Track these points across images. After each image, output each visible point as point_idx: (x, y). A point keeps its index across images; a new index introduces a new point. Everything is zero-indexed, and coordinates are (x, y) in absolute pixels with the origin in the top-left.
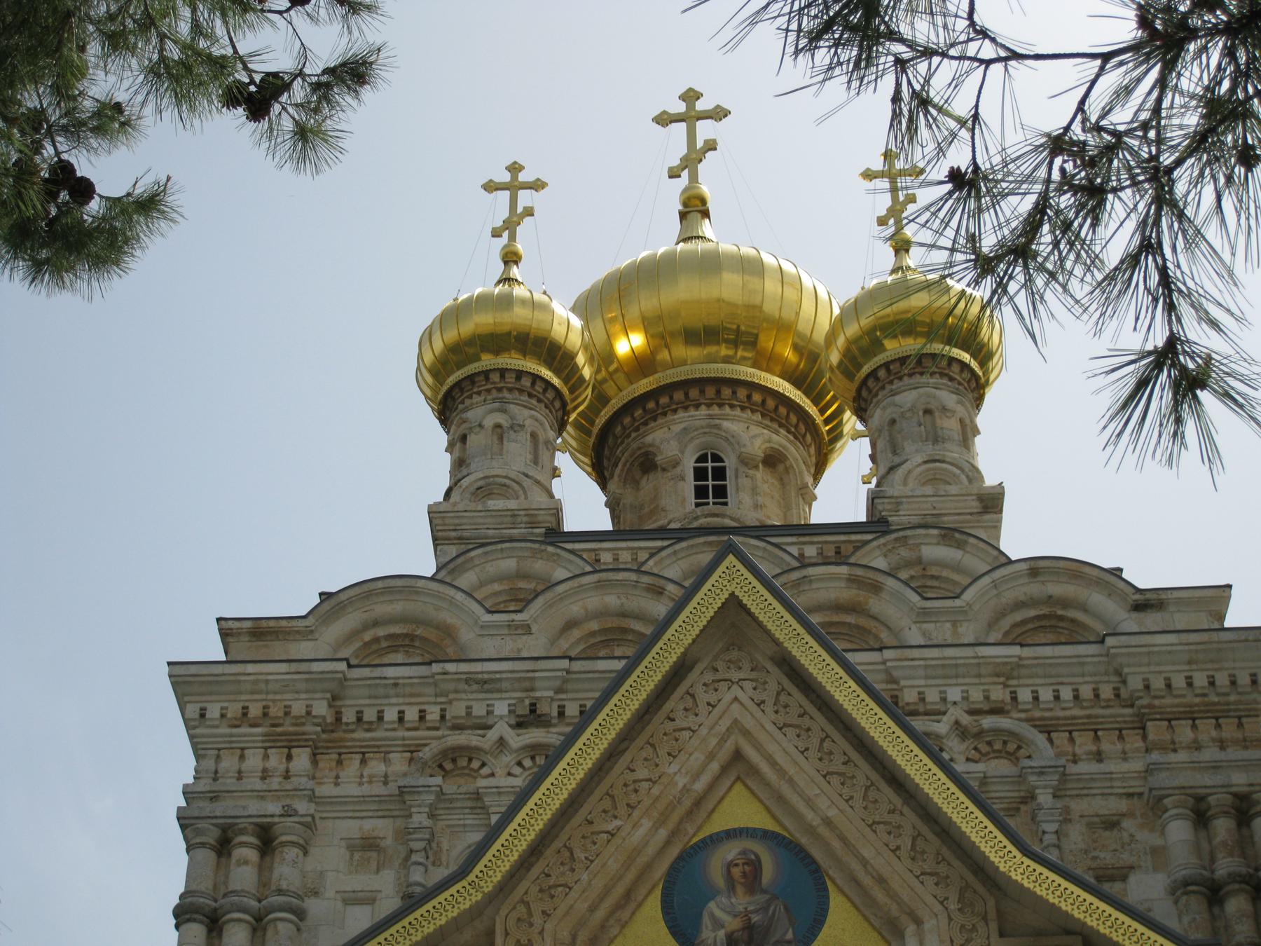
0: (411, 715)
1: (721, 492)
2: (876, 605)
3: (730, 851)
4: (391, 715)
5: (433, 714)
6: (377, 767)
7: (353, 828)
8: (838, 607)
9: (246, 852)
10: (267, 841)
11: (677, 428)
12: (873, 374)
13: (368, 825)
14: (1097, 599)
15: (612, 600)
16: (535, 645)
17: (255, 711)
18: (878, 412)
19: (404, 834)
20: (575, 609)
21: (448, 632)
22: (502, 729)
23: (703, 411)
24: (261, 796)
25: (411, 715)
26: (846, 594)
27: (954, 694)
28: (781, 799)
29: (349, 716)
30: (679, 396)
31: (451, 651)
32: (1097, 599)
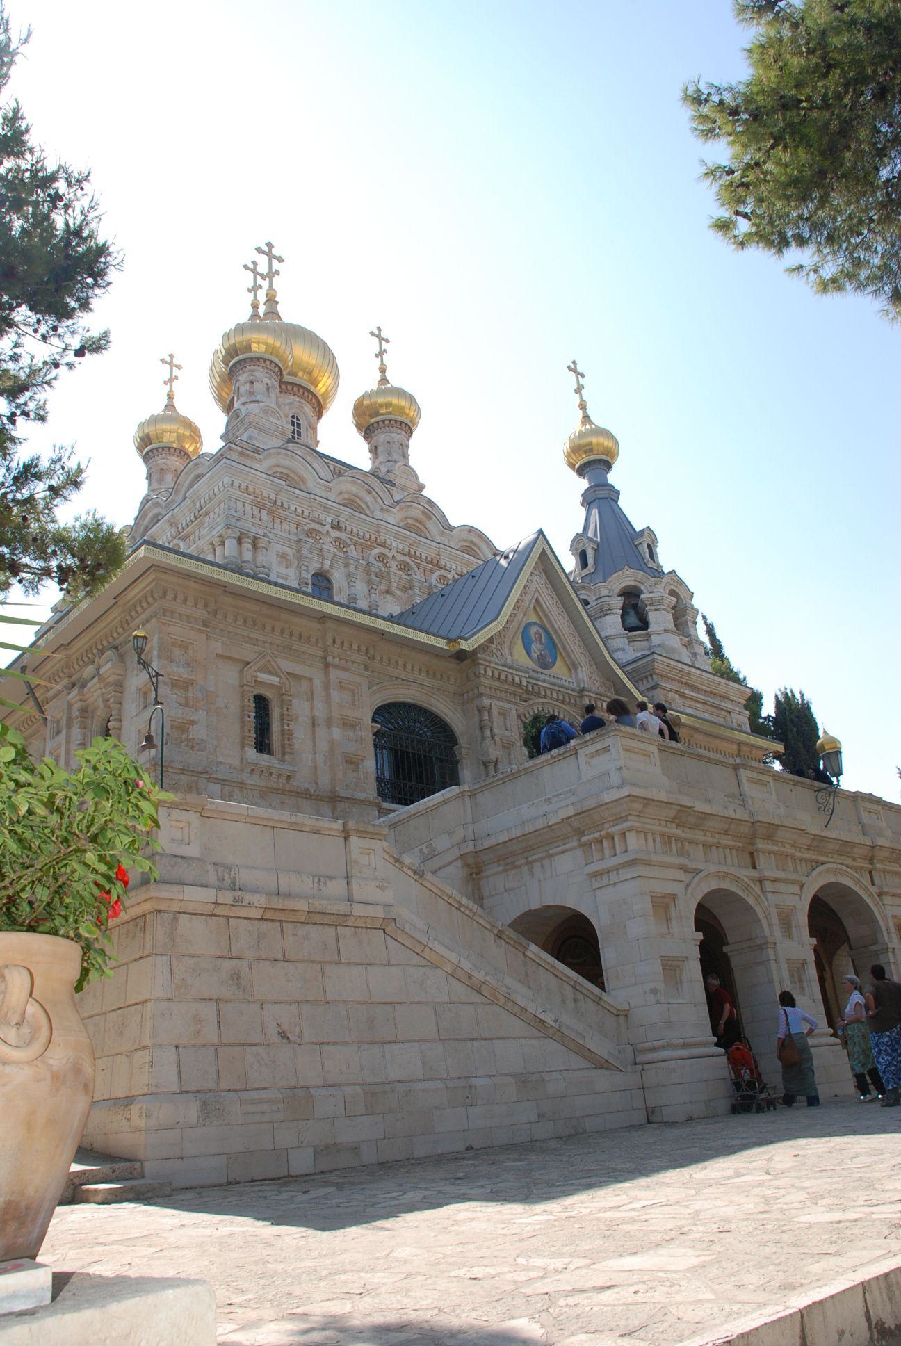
0: (299, 510)
1: (299, 434)
2: (429, 524)
3: (534, 629)
4: (292, 508)
5: (306, 514)
6: (285, 526)
7: (278, 547)
8: (417, 520)
9: (247, 546)
10: (254, 546)
11: (288, 401)
12: (383, 421)
13: (285, 548)
14: (484, 546)
15: (354, 489)
16: (332, 496)
17: (251, 489)
18: (383, 436)
19: (300, 558)
20: (343, 488)
21: (303, 480)
22: (328, 527)
23: (296, 398)
24: (254, 525)
25: (299, 510)
26: (421, 517)
27: (454, 566)
28: (546, 616)
29: (279, 503)
30: (290, 388)
31: (303, 487)
32: (484, 546)
